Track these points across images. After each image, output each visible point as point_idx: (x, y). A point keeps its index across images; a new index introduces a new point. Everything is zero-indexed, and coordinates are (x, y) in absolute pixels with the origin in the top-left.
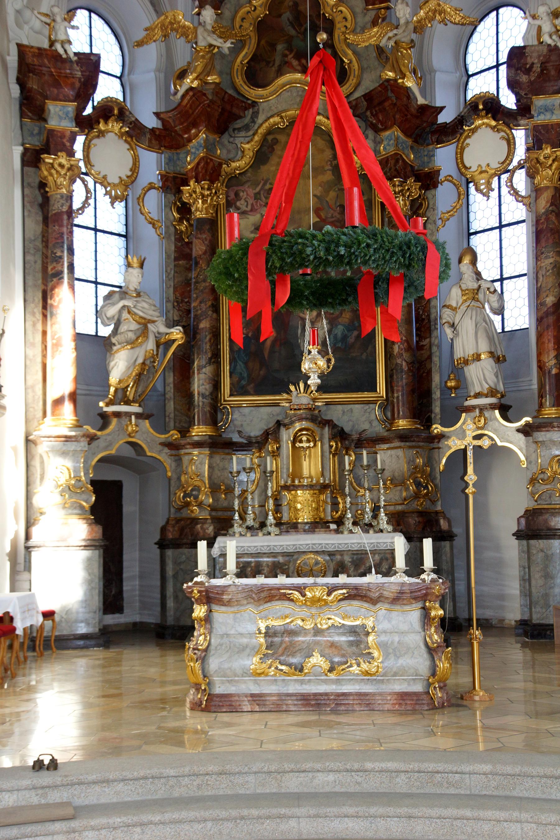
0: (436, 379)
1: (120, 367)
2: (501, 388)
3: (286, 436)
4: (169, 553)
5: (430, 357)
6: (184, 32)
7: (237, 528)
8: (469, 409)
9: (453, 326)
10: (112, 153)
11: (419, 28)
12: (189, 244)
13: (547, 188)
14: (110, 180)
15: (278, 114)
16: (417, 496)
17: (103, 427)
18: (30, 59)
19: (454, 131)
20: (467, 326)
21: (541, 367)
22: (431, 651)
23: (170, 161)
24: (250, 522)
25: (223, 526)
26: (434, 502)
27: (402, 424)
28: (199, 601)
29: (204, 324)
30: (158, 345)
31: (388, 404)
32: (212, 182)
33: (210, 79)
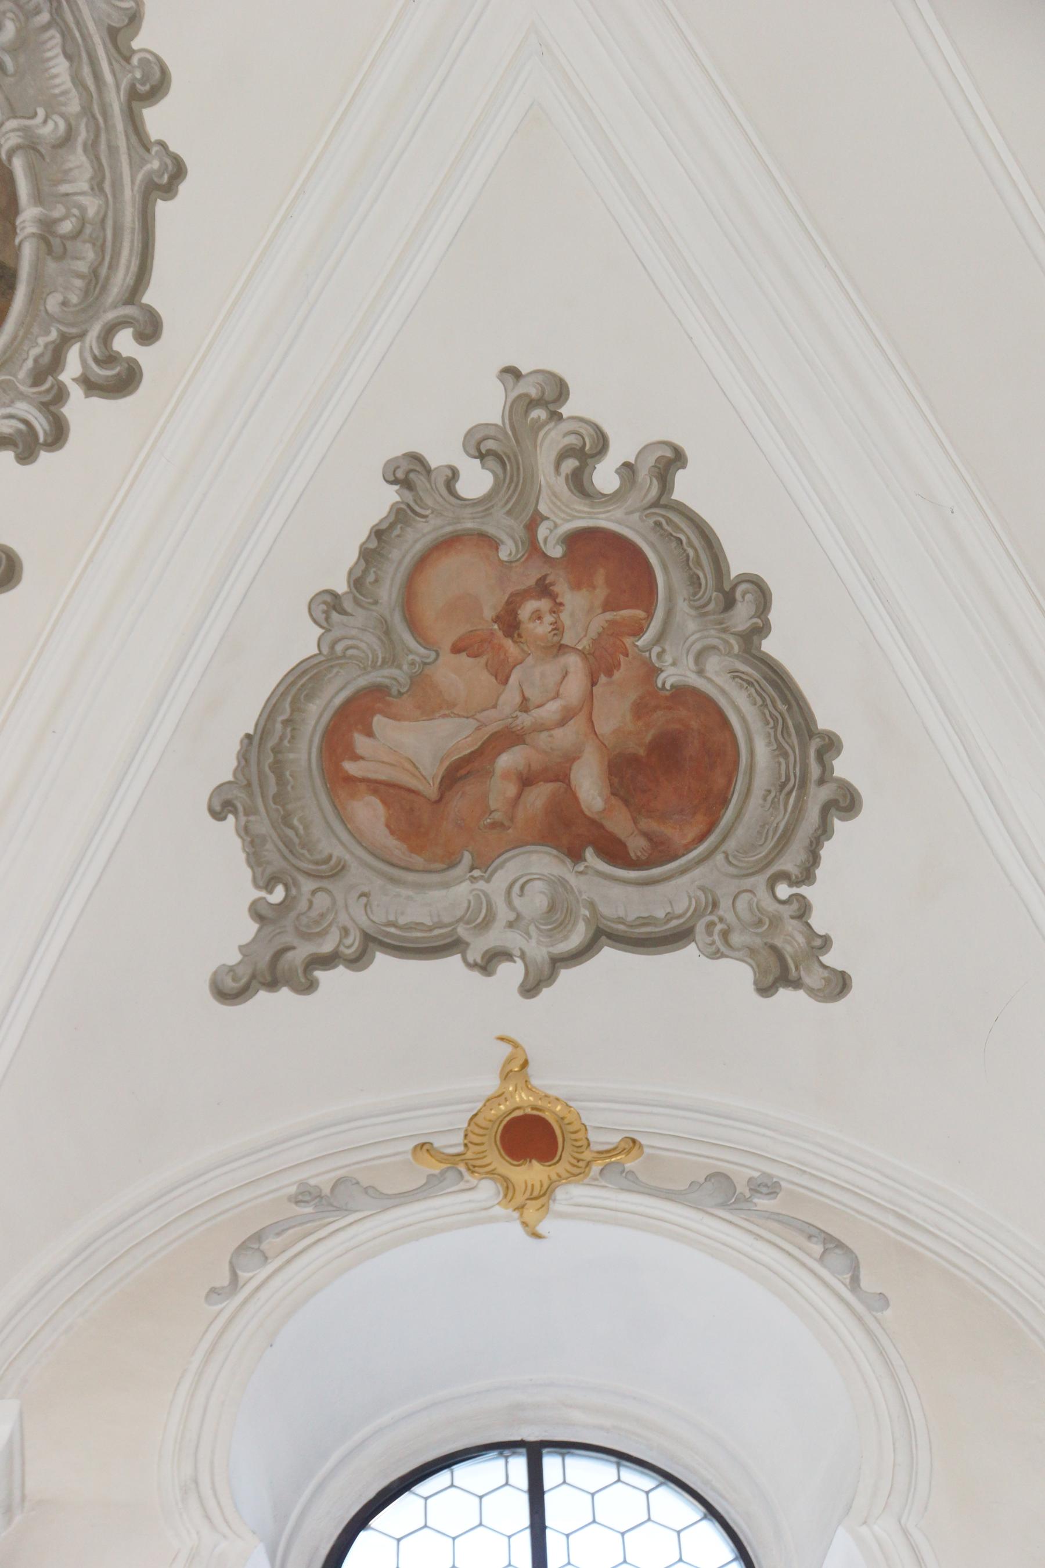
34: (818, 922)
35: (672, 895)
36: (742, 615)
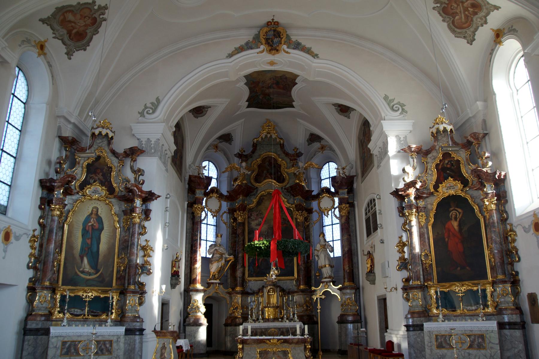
0: (313, 272)
1: (214, 268)
2: (333, 275)
3: (265, 290)
4: (229, 328)
5: (311, 266)
6: (237, 169)
7: (250, 320)
8: (323, 282)
9: (318, 256)
10: (214, 203)
11: (306, 169)
12: (236, 229)
13: (344, 216)
14: (213, 210)
15: (264, 191)
16: (307, 310)
17: (208, 287)
18: (192, 179)
20: (322, 256)
21: (344, 270)
23: (231, 205)
24: (254, 318)
25: (245, 319)
26: (312, 312)
27: (302, 287)
28: (240, 343)
29: (240, 255)
30: (226, 261)
31: (298, 280)
32: (244, 211)
33: (244, 182)
34: (74, 54)
35: (69, 42)
36: (95, 33)
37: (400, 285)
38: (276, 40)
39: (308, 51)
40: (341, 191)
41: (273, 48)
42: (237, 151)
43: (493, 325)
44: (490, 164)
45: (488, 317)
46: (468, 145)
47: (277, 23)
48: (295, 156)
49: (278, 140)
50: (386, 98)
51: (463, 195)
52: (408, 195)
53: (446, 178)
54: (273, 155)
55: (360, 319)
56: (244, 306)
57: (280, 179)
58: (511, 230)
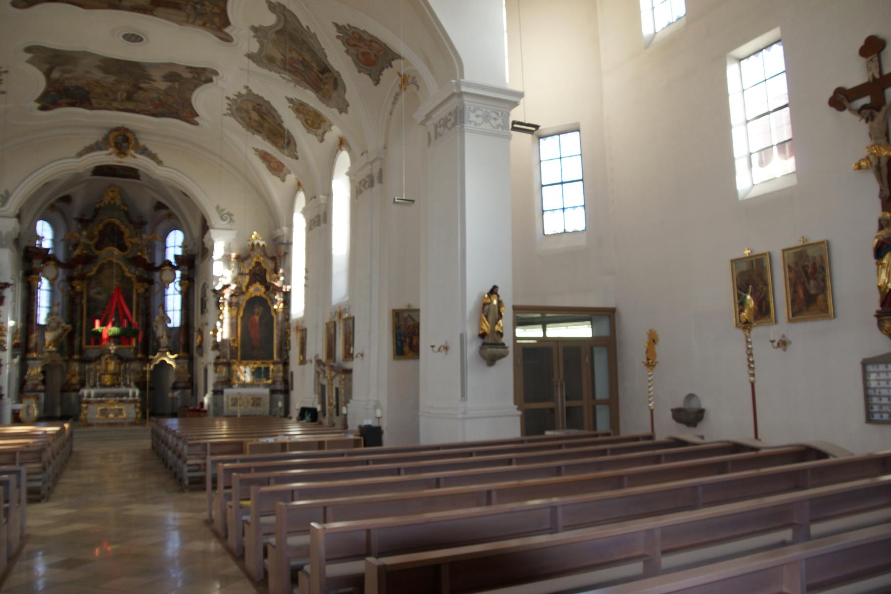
0: (151, 341)
4: (66, 394)
10: (51, 269)
19: (159, 269)
22: (137, 413)
25: (83, 384)
27: (139, 356)
29: (78, 324)
31: (136, 349)
37: (213, 361)
38: (125, 145)
39: (153, 157)
40: (183, 267)
41: (122, 152)
42: (76, 214)
43: (267, 391)
44: (282, 278)
45: (267, 386)
46: (273, 259)
47: (126, 130)
48: (139, 225)
49: (122, 207)
50: (218, 208)
51: (264, 296)
52: (223, 295)
53: (255, 282)
54: (117, 222)
55: (190, 384)
56: (82, 373)
57: (122, 248)
58: (289, 328)
